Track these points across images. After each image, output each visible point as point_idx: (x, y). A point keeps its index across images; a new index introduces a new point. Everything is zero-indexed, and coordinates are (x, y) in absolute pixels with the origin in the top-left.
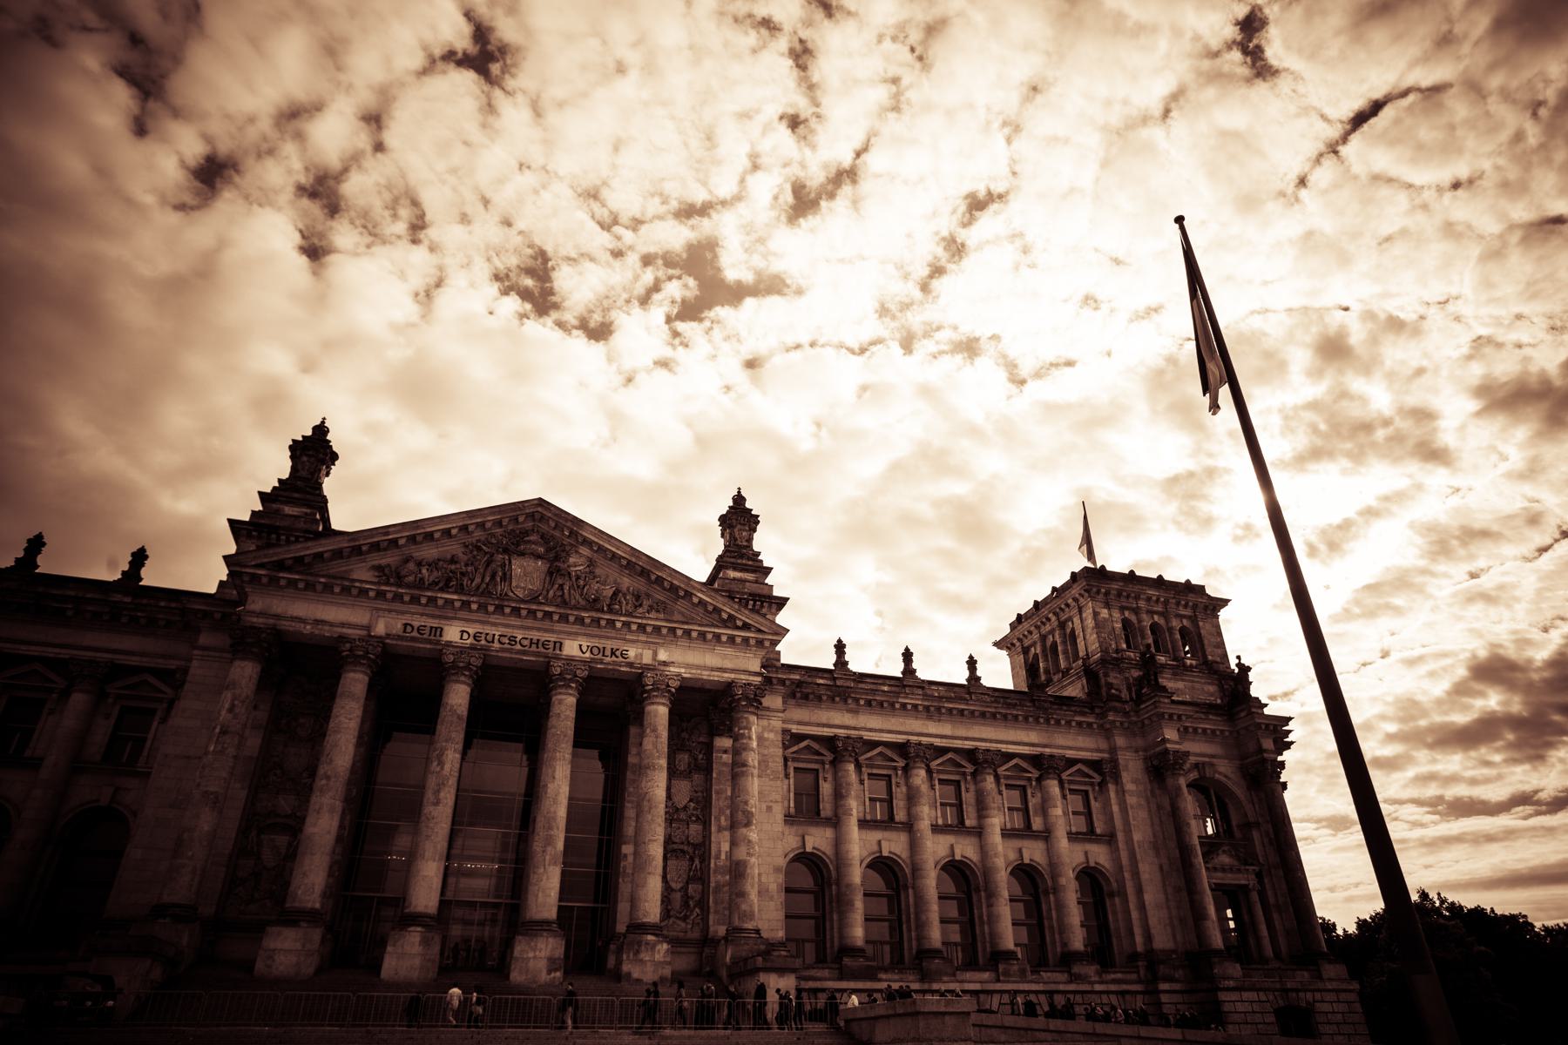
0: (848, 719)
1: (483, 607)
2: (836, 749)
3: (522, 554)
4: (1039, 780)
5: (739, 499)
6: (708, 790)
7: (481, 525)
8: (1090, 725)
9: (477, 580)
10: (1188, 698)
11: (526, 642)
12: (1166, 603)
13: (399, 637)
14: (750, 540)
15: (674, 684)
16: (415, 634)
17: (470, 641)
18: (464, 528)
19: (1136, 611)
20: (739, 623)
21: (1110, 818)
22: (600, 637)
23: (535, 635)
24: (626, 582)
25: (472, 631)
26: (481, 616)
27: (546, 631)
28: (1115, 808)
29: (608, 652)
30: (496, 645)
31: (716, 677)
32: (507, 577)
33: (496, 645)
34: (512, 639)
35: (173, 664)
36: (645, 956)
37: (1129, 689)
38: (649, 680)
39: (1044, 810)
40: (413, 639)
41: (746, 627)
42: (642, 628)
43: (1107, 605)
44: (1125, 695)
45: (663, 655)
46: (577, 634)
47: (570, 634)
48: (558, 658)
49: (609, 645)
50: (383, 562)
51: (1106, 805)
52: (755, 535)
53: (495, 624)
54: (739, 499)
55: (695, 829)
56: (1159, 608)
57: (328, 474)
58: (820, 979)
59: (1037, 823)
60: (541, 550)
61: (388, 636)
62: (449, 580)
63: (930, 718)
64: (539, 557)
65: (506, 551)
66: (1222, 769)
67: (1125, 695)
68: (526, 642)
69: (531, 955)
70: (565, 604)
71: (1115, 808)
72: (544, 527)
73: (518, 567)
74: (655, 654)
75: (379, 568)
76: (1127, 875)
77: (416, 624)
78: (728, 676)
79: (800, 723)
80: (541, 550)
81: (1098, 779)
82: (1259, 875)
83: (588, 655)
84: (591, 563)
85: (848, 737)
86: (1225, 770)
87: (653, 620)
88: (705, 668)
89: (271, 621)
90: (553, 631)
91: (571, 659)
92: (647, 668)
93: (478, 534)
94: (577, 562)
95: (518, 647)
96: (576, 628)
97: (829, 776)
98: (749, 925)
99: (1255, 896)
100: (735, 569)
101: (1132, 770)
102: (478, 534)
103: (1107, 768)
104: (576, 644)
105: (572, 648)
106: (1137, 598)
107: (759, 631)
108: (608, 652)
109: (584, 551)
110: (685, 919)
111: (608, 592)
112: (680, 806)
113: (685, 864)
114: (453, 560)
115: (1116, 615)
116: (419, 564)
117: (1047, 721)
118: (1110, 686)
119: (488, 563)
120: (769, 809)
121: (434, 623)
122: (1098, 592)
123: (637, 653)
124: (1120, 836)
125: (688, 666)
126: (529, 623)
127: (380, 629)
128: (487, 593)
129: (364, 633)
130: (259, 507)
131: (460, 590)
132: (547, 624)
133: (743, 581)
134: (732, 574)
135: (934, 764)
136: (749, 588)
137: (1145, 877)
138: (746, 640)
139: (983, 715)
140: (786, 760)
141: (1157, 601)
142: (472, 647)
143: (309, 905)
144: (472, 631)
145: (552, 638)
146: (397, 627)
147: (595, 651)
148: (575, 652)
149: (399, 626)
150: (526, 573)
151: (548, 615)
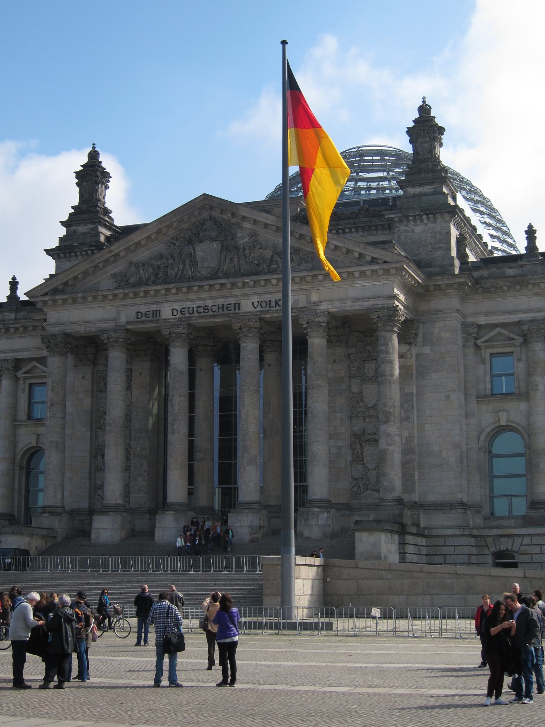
3: (201, 241)
5: (424, 109)
7: (169, 226)
9: (176, 269)
11: (215, 309)
13: (135, 322)
15: (323, 319)
16: (144, 318)
17: (179, 315)
18: (159, 232)
20: (369, 259)
22: (265, 293)
25: (179, 309)
27: (227, 297)
29: (273, 304)
30: (196, 314)
31: (357, 306)
32: (194, 262)
33: (196, 314)
34: (206, 308)
36: (312, 522)
40: (143, 322)
41: (374, 261)
45: (314, 297)
46: (248, 295)
47: (243, 296)
50: (117, 270)
53: (192, 300)
57: (107, 187)
58: (507, 527)
60: (214, 233)
61: (127, 323)
62: (156, 275)
64: (213, 240)
65: (190, 242)
68: (215, 309)
69: (238, 525)
74: (308, 297)
75: (115, 276)
77: (143, 311)
78: (366, 304)
79: (487, 314)
83: (259, 309)
85: (533, 321)
89: (62, 328)
90: (231, 296)
94: (243, 238)
95: (210, 313)
96: (246, 291)
98: (390, 496)
100: (414, 186)
104: (249, 302)
105: (247, 306)
107: (385, 262)
108: (273, 304)
111: (268, 254)
112: (370, 405)
116: (137, 266)
119: (181, 253)
120: (447, 397)
121: (154, 308)
127: (123, 319)
129: (112, 324)
130: (63, 231)
131: (164, 283)
133: (421, 195)
138: (374, 272)
143: (114, 502)
144: (179, 309)
145: (232, 301)
147: (264, 304)
148: (250, 308)
149: (134, 315)
151: (222, 285)
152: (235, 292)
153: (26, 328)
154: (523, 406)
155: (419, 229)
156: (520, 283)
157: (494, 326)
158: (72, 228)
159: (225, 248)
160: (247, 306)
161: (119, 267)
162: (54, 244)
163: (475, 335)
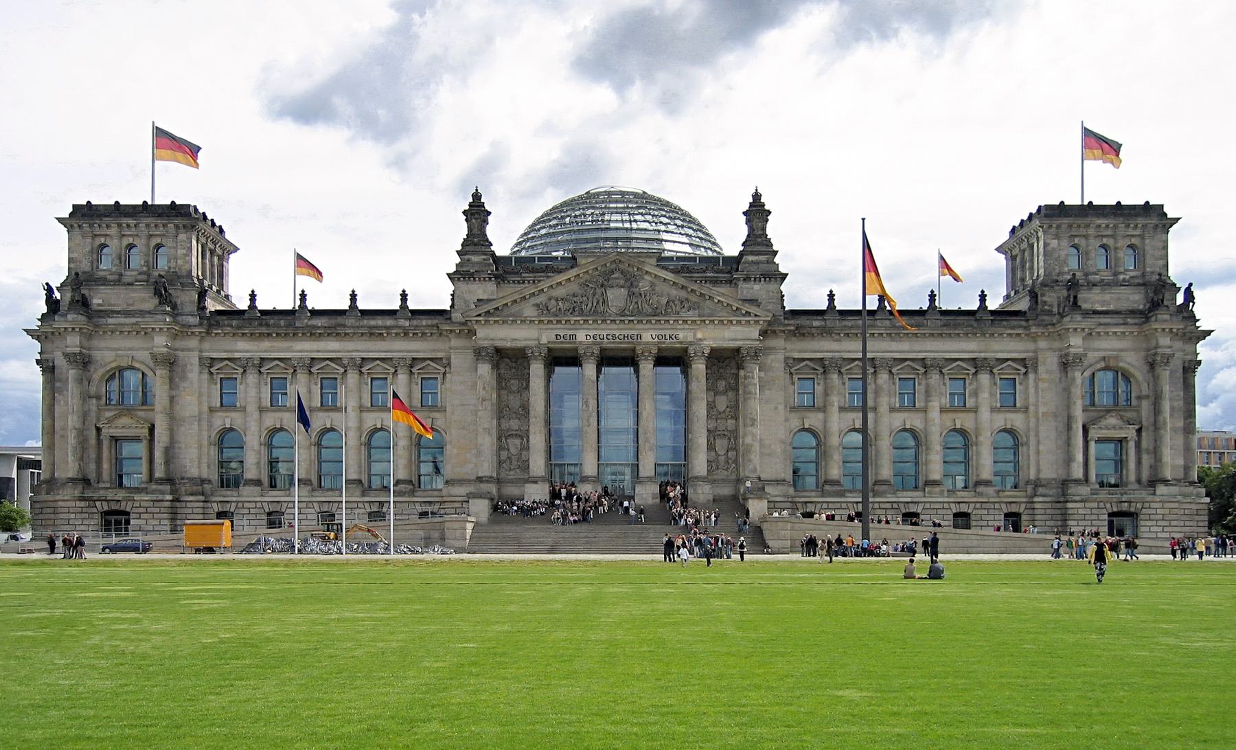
0: (834, 346)
1: (595, 321)
2: (823, 366)
4: (975, 374)
5: (757, 196)
6: (737, 401)
8: (1018, 335)
10: (1112, 307)
12: (1115, 227)
14: (764, 229)
19: (1086, 237)
21: (1027, 399)
23: (626, 333)
24: (674, 292)
26: (595, 326)
28: (1032, 390)
35: (440, 355)
37: (1059, 306)
38: (691, 351)
39: (975, 394)
42: (685, 322)
43: (1057, 237)
44: (1055, 310)
45: (699, 335)
48: (639, 344)
49: (668, 333)
51: (1027, 388)
52: (769, 225)
54: (757, 196)
55: (731, 422)
56: (1109, 232)
59: (970, 403)
63: (893, 339)
66: (1129, 360)
67: (1055, 310)
70: (640, 313)
71: (1032, 390)
72: (621, 266)
73: (611, 294)
74: (695, 335)
76: (1032, 434)
79: (800, 351)
80: (622, 282)
81: (1024, 370)
82: (1139, 431)
84: (652, 285)
86: (1132, 361)
87: (691, 315)
88: (724, 339)
91: (647, 343)
92: (691, 343)
93: (587, 277)
96: (648, 326)
97: (822, 382)
99: (1132, 445)
101: (1049, 363)
102: (587, 277)
103: (1029, 364)
105: (647, 337)
106: (1087, 226)
109: (647, 277)
110: (727, 470)
113: (725, 442)
114: (574, 295)
115: (1065, 243)
117: (983, 335)
118: (1045, 303)
120: (776, 408)
121: (571, 332)
122: (1050, 227)
123: (684, 335)
124: (1032, 409)
125: (714, 339)
126: (622, 326)
128: (596, 312)
131: (581, 313)
132: (631, 325)
133: (757, 263)
134: (750, 258)
135: (894, 370)
136: (764, 267)
137: (1042, 434)
139: (932, 335)
140: (791, 374)
141: (1107, 226)
142: (594, 344)
146: (553, 338)
150: (616, 297)
152: (640, 326)
153: (423, 334)
154: (821, 415)
155: (757, 287)
156: (826, 332)
157: (804, 360)
158: (467, 257)
159: (631, 295)
160: (647, 337)
161: (542, 299)
162: (453, 269)
163: (791, 364)
